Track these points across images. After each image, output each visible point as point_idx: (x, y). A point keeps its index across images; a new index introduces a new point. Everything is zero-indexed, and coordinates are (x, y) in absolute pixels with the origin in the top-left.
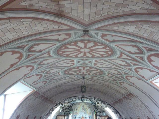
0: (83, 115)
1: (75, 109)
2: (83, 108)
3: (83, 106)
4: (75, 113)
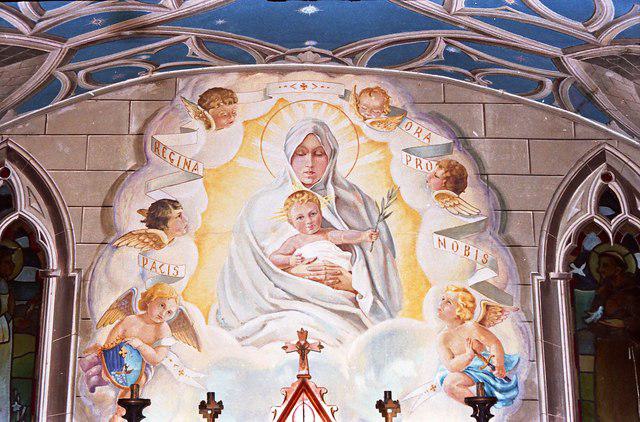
0: (303, 350)
1: (106, 206)
2: (307, 194)
3: (317, 150)
4: (103, 301)
